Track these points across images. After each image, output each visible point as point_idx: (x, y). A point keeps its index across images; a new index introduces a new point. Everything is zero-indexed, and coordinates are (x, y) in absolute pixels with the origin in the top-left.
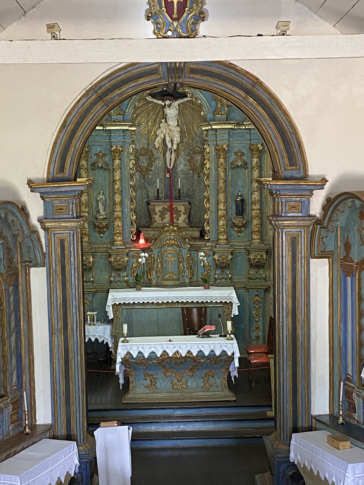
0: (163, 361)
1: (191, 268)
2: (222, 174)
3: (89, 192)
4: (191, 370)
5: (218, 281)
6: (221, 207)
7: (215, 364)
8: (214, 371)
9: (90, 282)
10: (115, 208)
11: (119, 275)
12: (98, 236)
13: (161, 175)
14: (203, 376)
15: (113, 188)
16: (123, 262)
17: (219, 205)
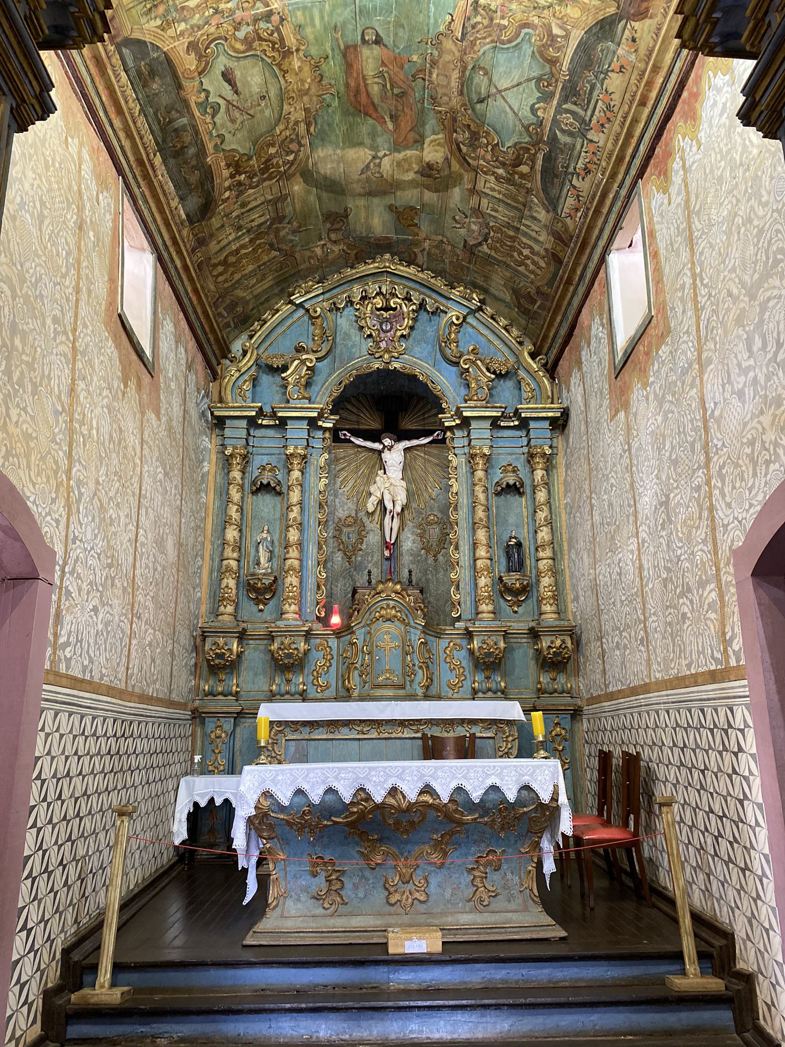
0: (362, 815)
1: (427, 667)
2: (481, 497)
3: (244, 528)
4: (437, 845)
5: (480, 695)
6: (482, 552)
7: (502, 829)
8: (499, 851)
9: (231, 694)
10: (288, 552)
11: (289, 681)
12: (254, 609)
13: (377, 557)
14: (471, 866)
15: (288, 520)
16: (296, 649)
17: (478, 550)
